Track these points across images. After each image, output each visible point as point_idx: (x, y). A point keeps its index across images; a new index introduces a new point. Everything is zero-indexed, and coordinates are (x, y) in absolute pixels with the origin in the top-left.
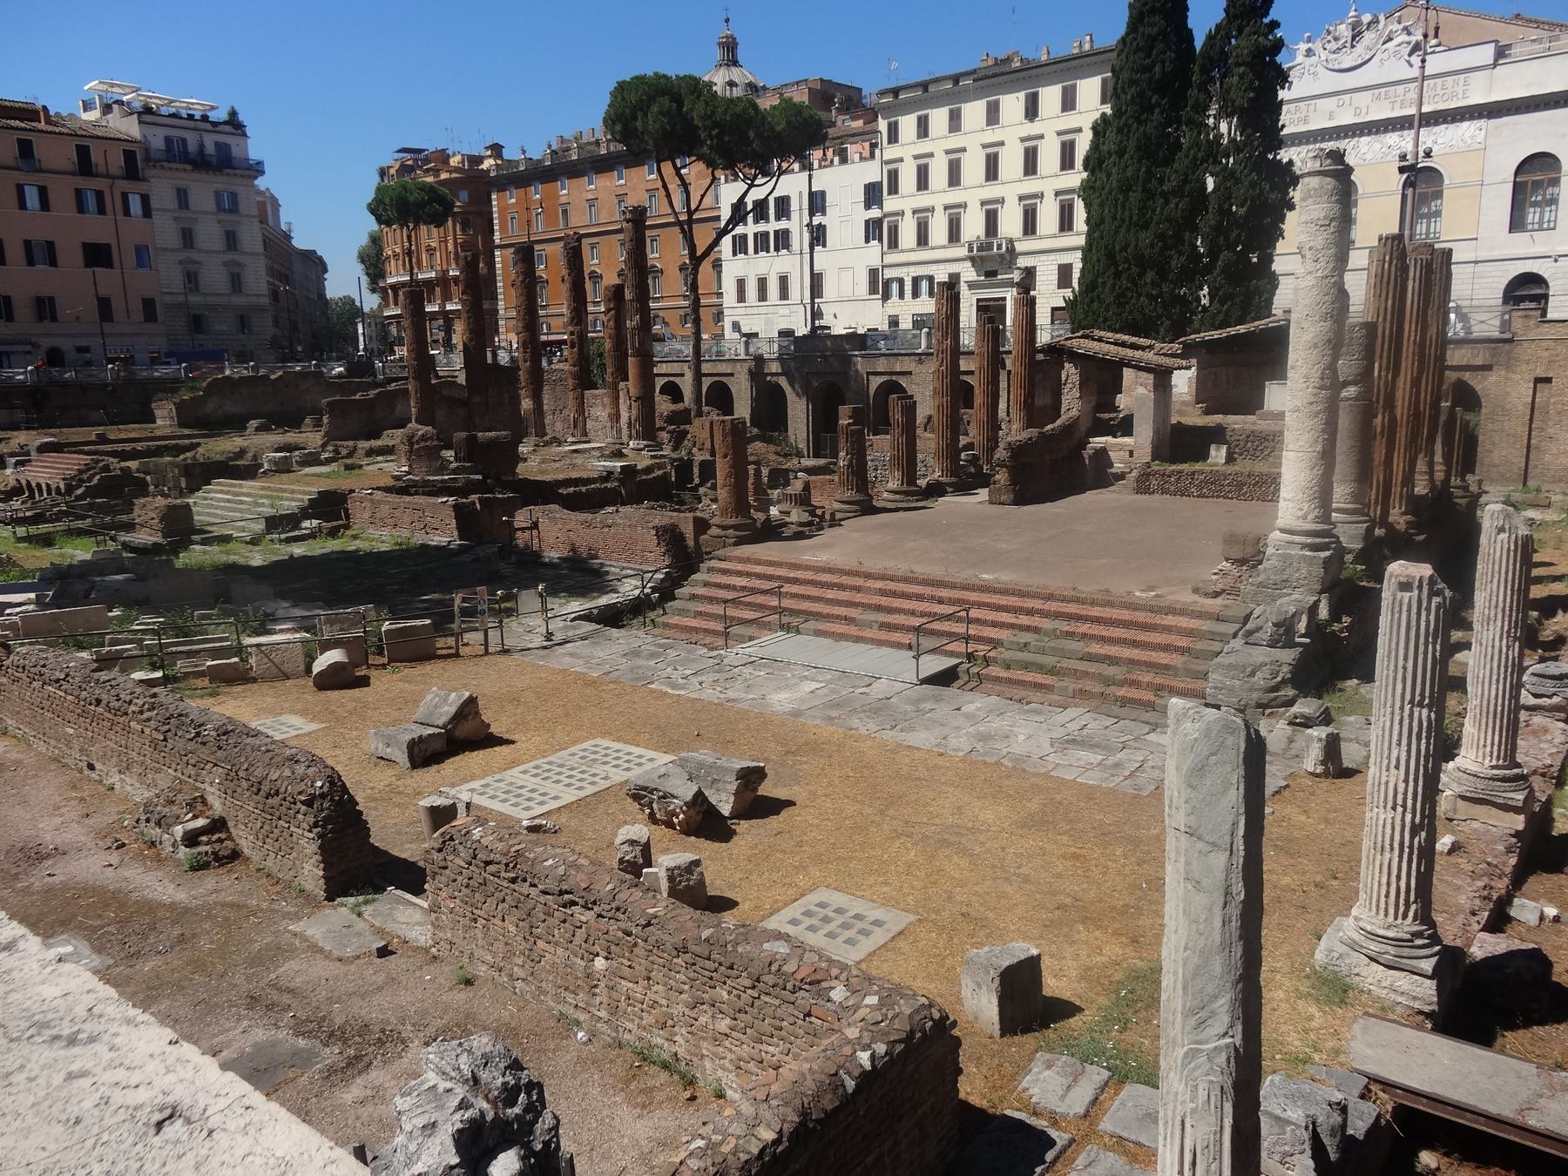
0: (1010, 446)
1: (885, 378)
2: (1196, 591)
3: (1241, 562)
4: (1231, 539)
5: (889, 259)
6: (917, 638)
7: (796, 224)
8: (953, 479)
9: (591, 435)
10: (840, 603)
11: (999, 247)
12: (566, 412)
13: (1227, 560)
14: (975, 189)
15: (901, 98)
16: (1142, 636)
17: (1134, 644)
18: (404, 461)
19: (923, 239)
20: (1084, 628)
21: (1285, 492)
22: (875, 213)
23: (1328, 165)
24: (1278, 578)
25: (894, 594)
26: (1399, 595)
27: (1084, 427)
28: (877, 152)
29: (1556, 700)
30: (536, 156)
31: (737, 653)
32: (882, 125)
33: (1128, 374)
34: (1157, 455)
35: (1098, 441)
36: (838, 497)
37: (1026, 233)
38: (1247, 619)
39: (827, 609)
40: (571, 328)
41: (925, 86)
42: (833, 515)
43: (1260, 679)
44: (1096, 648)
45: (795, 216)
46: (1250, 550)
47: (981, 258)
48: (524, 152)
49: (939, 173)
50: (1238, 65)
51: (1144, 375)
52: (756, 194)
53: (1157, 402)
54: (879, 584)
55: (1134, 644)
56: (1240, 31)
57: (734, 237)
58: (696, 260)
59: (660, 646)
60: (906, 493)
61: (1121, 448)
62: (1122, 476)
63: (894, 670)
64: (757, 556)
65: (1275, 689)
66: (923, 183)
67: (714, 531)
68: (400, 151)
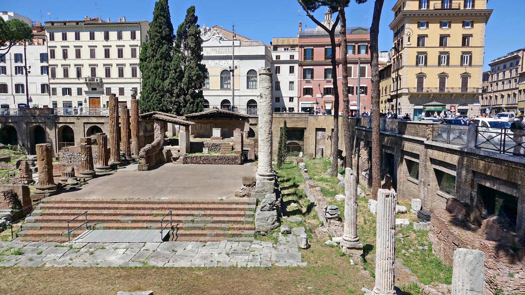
1: (64, 125)
2: (236, 196)
3: (249, 186)
4: (245, 179)
5: (52, 81)
8: (119, 162)
10: (110, 215)
11: (97, 80)
14: (86, 60)
15: (53, 26)
16: (228, 212)
17: (227, 215)
19: (66, 74)
20: (208, 212)
22: (45, 64)
23: (267, 72)
24: (262, 190)
25: (133, 209)
26: (386, 198)
27: (162, 143)
28: (45, 43)
29: (336, 215)
31: (77, 243)
32: (48, 35)
33: (170, 125)
36: (81, 172)
37: (106, 76)
39: (106, 218)
41: (65, 23)
42: (84, 179)
43: (270, 221)
44: (215, 219)
45: (8, 62)
46: (251, 182)
47: (90, 83)
50: (190, 35)
51: (182, 127)
53: (186, 135)
54: (125, 206)
56: (190, 27)
59: (34, 245)
60: (106, 169)
62: (178, 158)
63: (153, 238)
64: (64, 200)
65: (273, 224)
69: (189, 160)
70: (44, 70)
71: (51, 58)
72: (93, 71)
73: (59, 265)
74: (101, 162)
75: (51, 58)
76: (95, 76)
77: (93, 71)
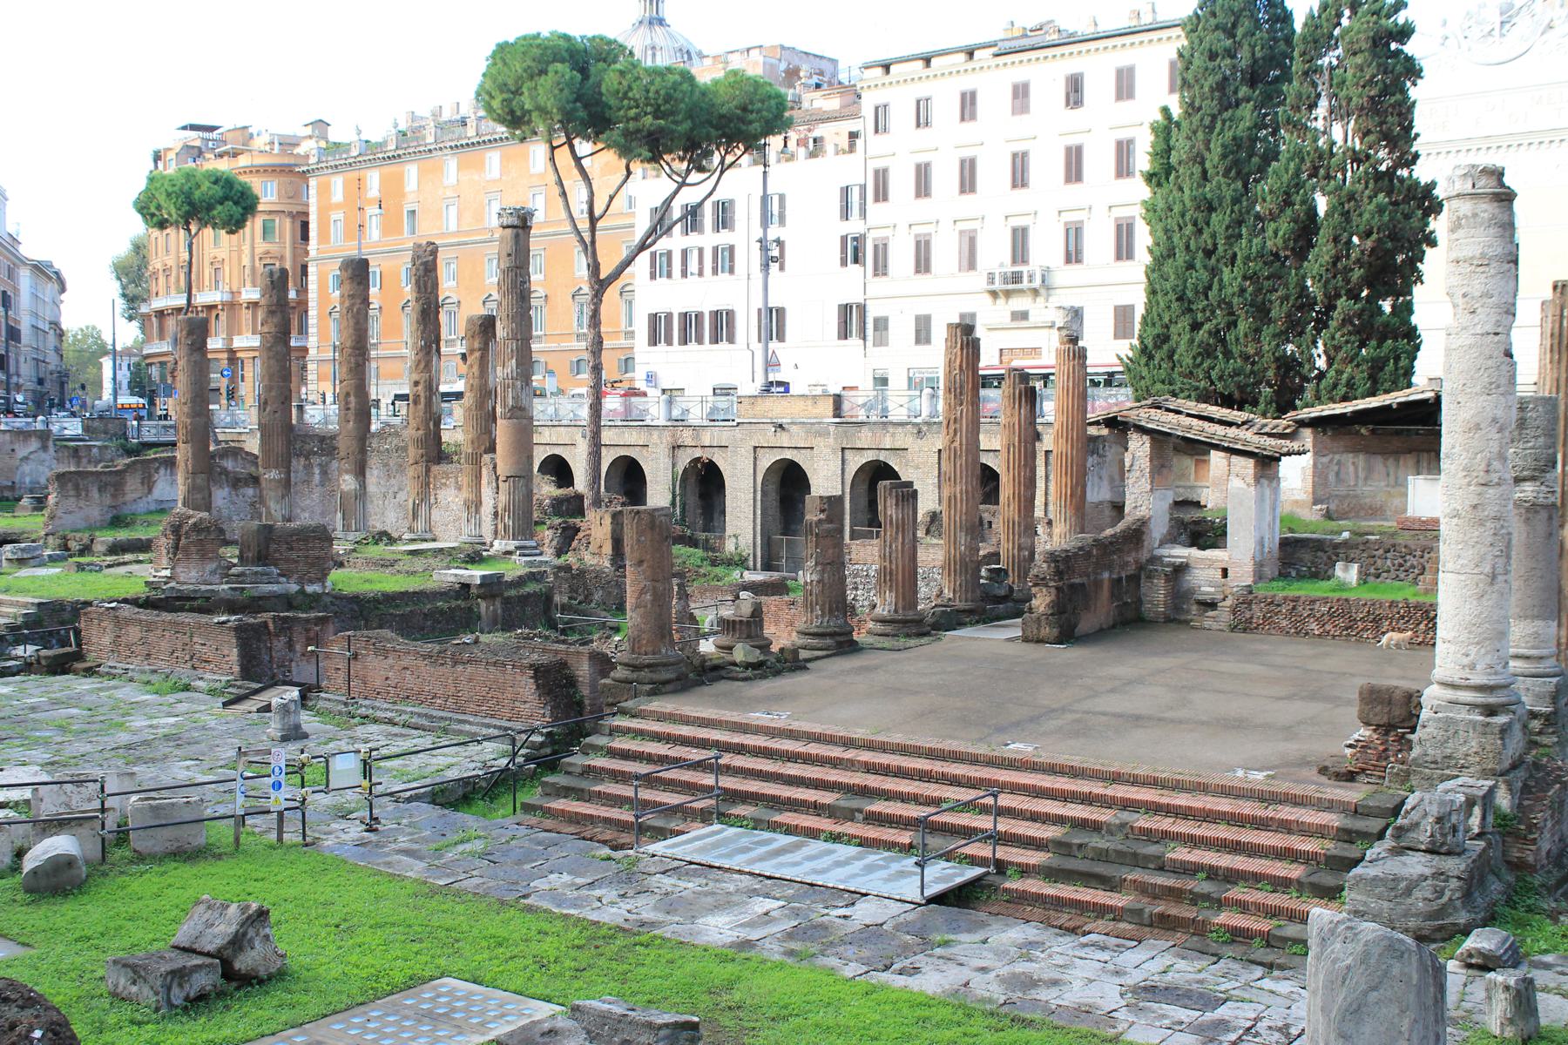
0: (1052, 557)
4: (1374, 698)
6: (928, 836)
7: (744, 235)
9: (438, 531)
12: (402, 496)
13: (1367, 724)
18: (165, 561)
19: (923, 264)
21: (1444, 630)
22: (854, 226)
28: (859, 142)
30: (375, 138)
34: (1259, 576)
35: (1180, 553)
38: (1396, 811)
40: (415, 377)
43: (1419, 901)
46: (1398, 712)
48: (359, 132)
49: (945, 178)
51: (1237, 460)
52: (689, 196)
55: (1236, 848)
57: (653, 255)
58: (600, 285)
61: (1211, 563)
66: (923, 187)
67: (620, 673)
68: (184, 128)
69: (1258, 611)
70: (853, 251)
71: (877, 200)
72: (1020, 239)
73: (559, 906)
74: (890, 597)
75: (877, 200)
76: (1025, 261)
77: (1020, 239)
